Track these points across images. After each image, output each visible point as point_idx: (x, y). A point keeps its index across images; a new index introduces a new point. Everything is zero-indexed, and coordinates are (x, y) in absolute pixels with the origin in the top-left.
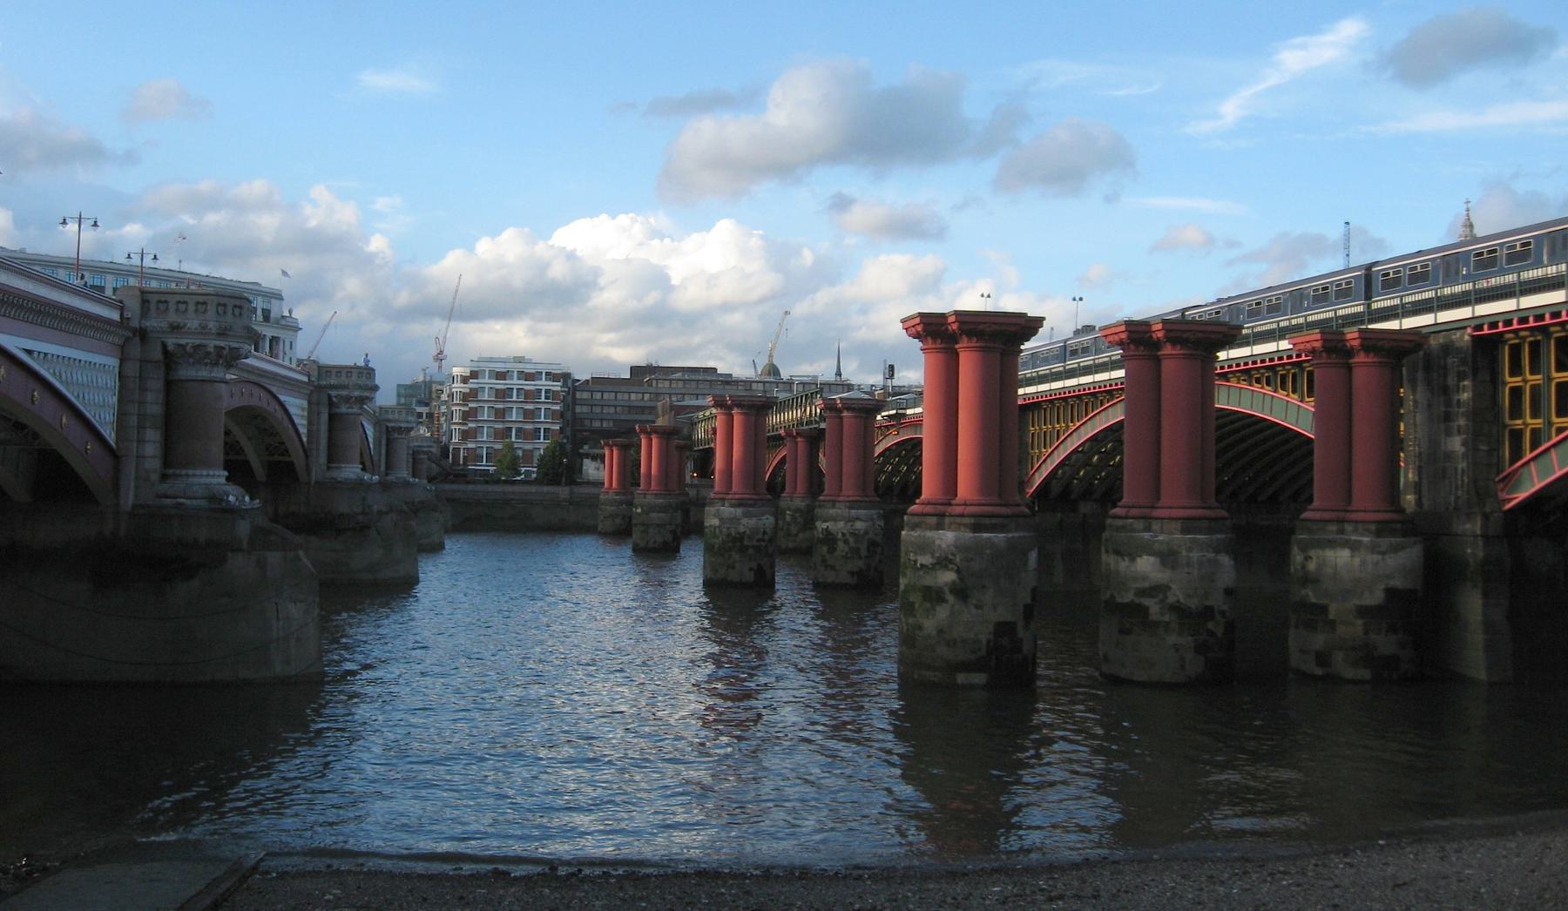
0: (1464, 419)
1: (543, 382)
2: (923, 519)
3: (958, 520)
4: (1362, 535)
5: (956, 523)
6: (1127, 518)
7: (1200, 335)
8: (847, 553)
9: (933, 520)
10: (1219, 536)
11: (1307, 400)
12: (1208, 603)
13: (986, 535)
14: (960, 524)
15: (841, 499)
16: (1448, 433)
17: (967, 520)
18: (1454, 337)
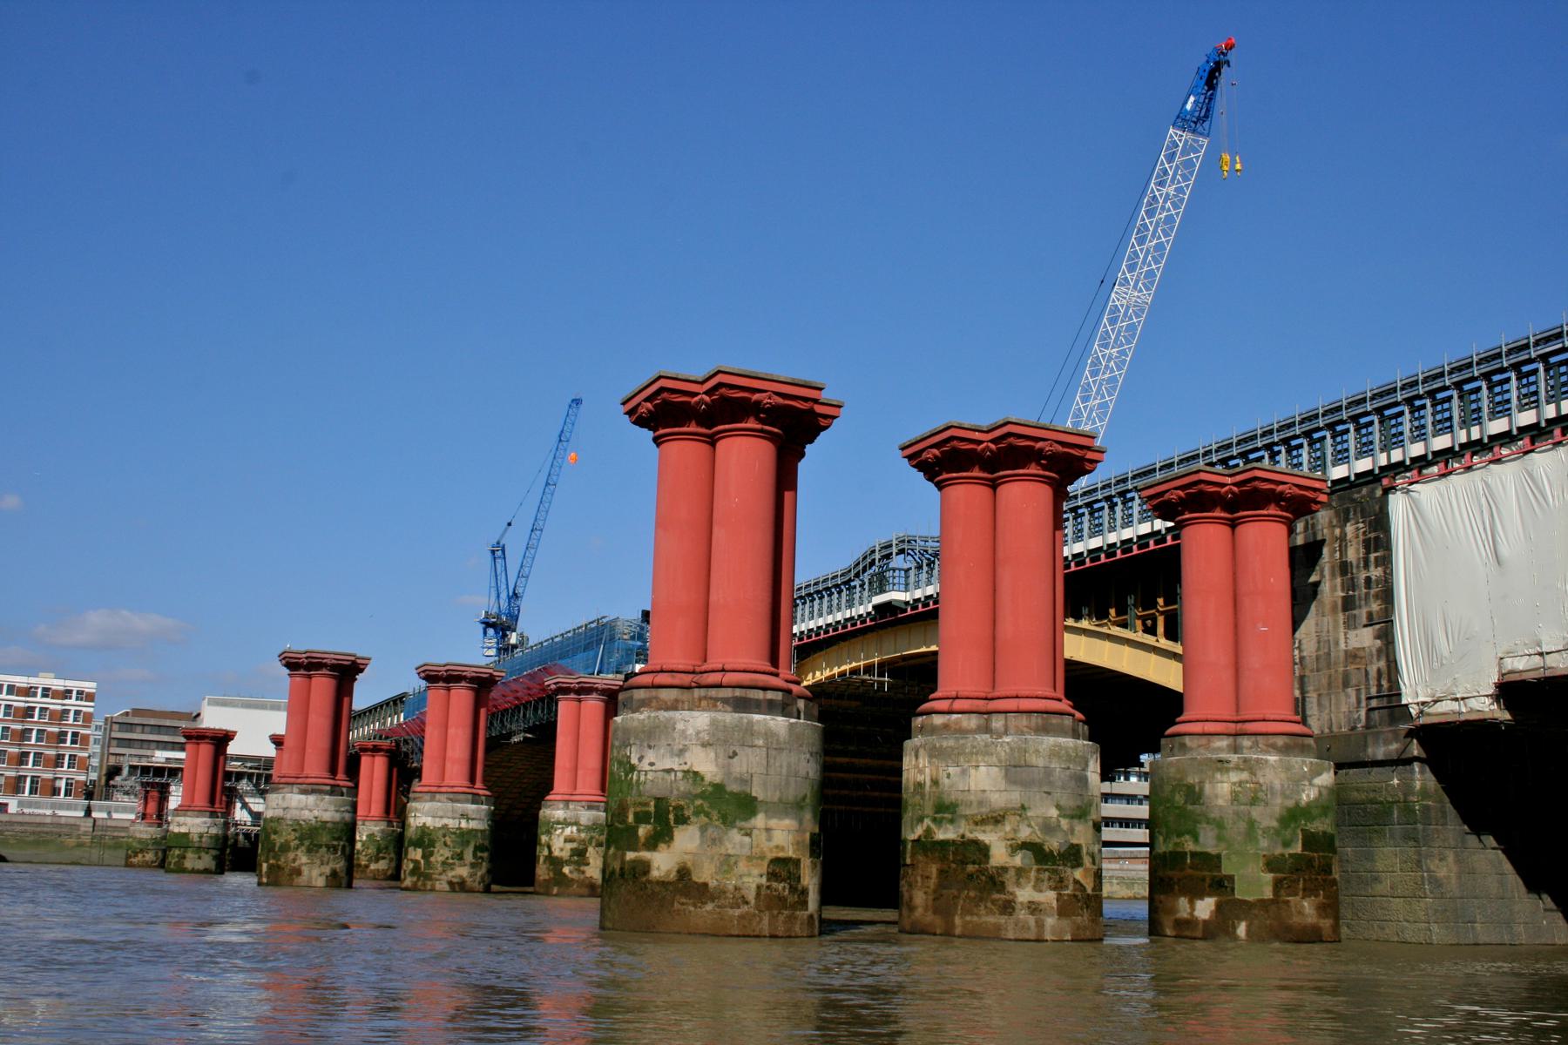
0: (1379, 602)
1: (73, 701)
2: (654, 692)
3: (713, 692)
4: (1267, 752)
5: (711, 698)
6: (950, 712)
8: (447, 858)
12: (1075, 841)
13: (757, 717)
14: (716, 699)
16: (1350, 624)
17: (726, 693)
18: (1356, 496)
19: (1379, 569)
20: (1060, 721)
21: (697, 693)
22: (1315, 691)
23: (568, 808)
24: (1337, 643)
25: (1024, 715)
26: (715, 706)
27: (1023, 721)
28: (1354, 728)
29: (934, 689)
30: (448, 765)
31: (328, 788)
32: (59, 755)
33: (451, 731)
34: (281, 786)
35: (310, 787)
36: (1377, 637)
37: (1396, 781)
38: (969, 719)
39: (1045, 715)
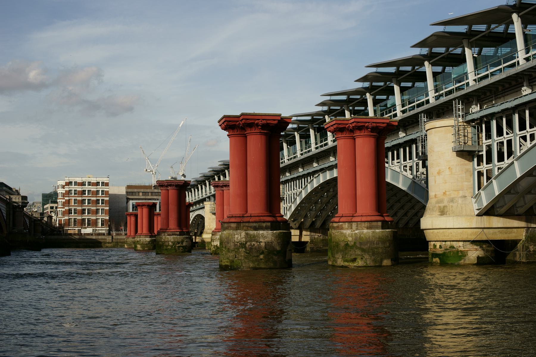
2: (229, 224)
3: (247, 224)
5: (246, 226)
6: (339, 222)
7: (375, 125)
9: (233, 225)
10: (387, 230)
14: (248, 227)
17: (252, 224)
20: (376, 224)
25: (363, 223)
26: (248, 229)
31: (178, 233)
32: (97, 209)
34: (161, 233)
38: (345, 224)
39: (370, 222)
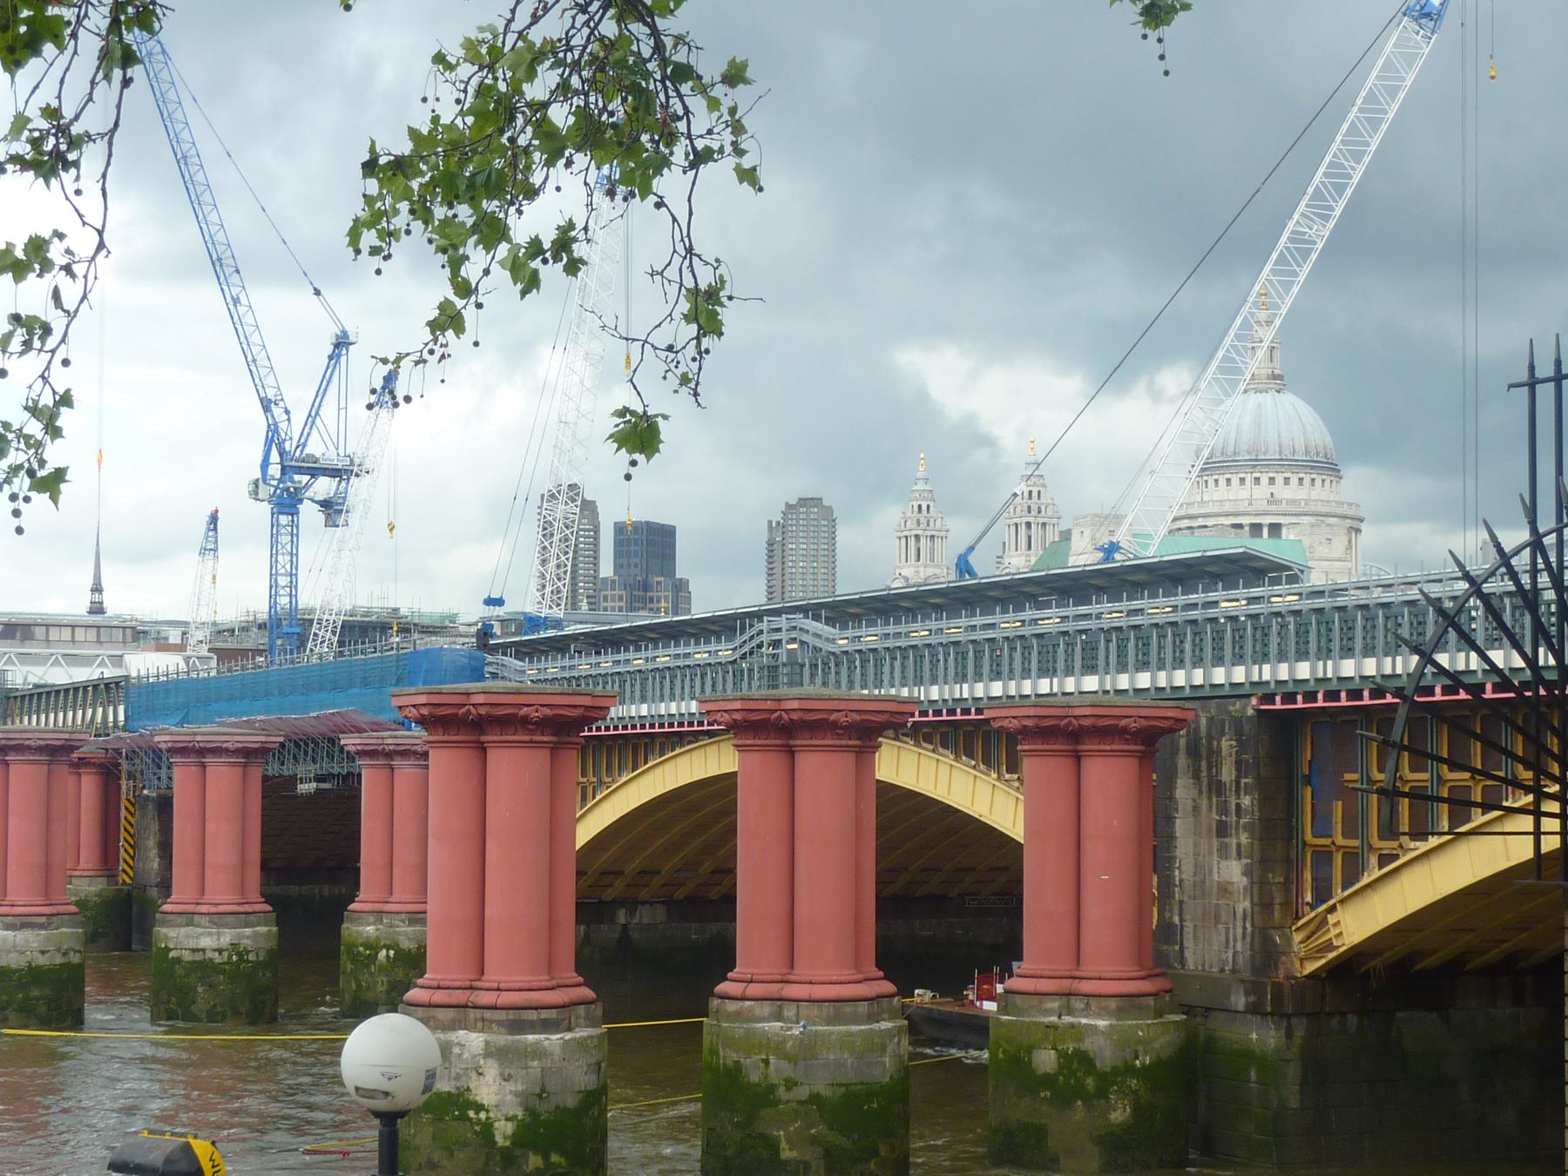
0: (1246, 835)
3: (488, 1014)
6: (743, 999)
8: (215, 1006)
11: (1007, 776)
13: (530, 1037)
14: (491, 1022)
15: (204, 909)
16: (1224, 853)
18: (1231, 708)
19: (1247, 797)
21: (473, 1014)
22: (1192, 921)
23: (381, 922)
24: (1211, 871)
26: (490, 1028)
27: (815, 1010)
28: (1222, 970)
29: (732, 966)
30: (209, 874)
33: (210, 826)
35: (18, 920)
36: (1245, 874)
37: (1254, 1036)
